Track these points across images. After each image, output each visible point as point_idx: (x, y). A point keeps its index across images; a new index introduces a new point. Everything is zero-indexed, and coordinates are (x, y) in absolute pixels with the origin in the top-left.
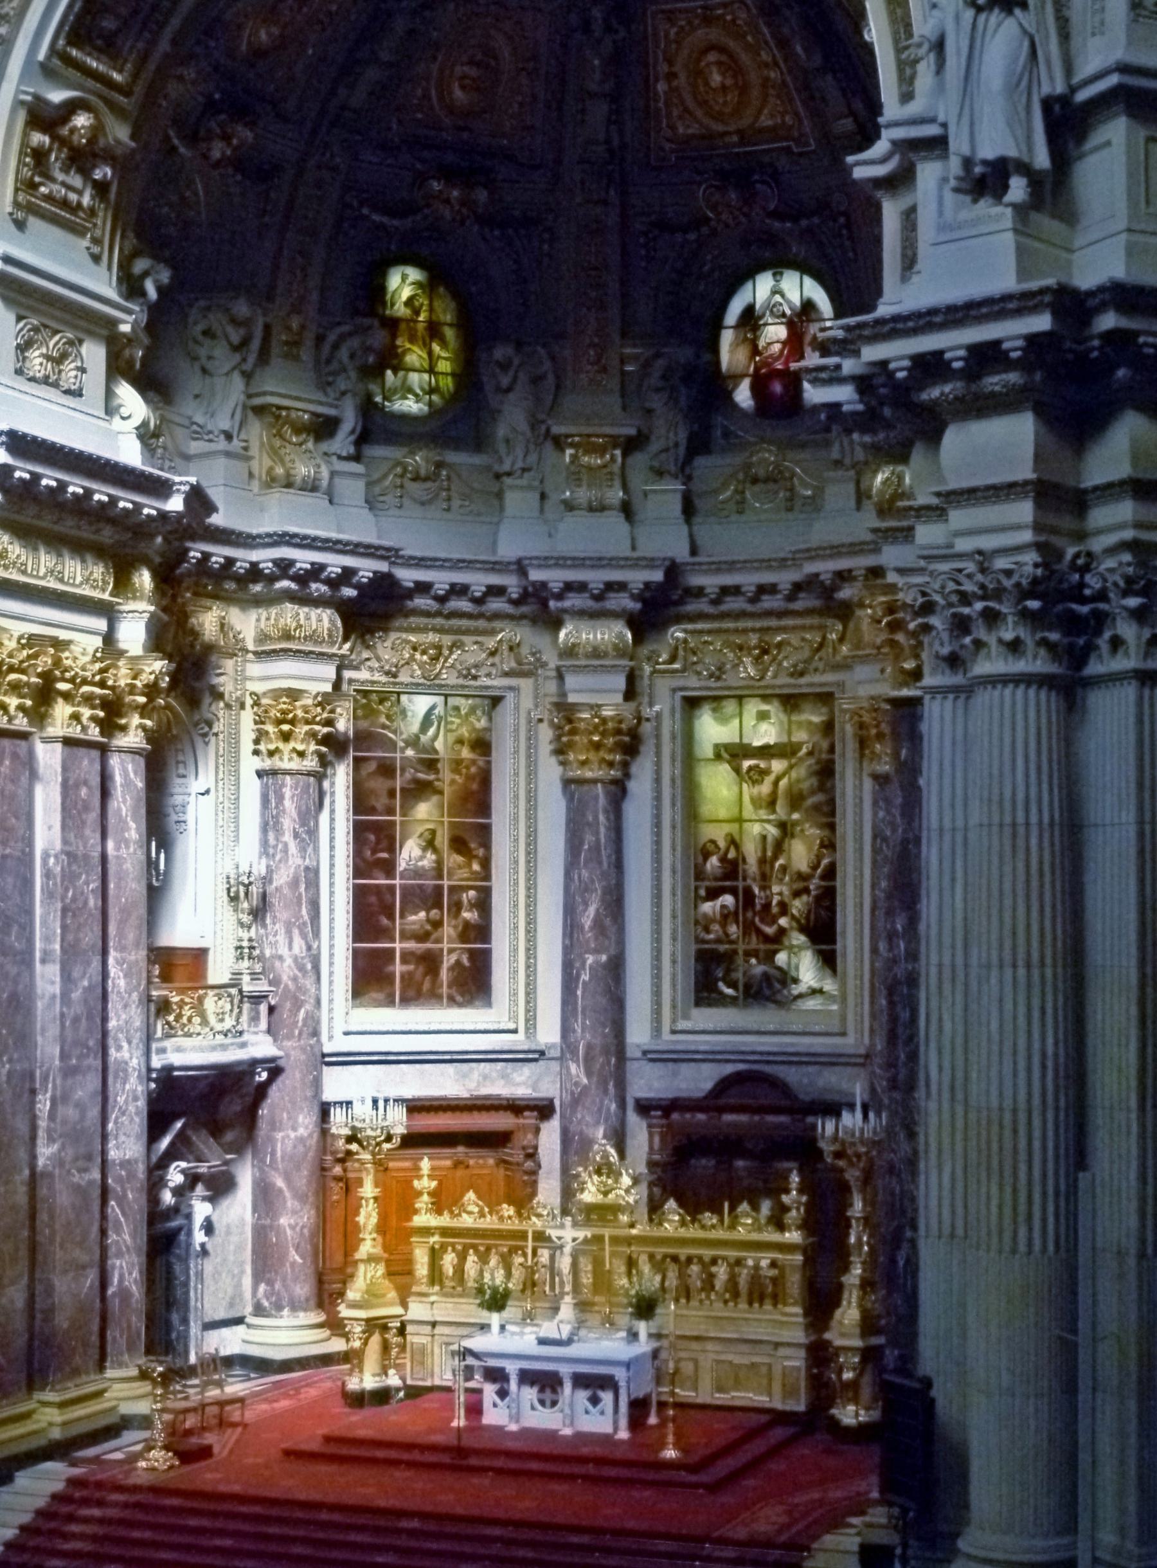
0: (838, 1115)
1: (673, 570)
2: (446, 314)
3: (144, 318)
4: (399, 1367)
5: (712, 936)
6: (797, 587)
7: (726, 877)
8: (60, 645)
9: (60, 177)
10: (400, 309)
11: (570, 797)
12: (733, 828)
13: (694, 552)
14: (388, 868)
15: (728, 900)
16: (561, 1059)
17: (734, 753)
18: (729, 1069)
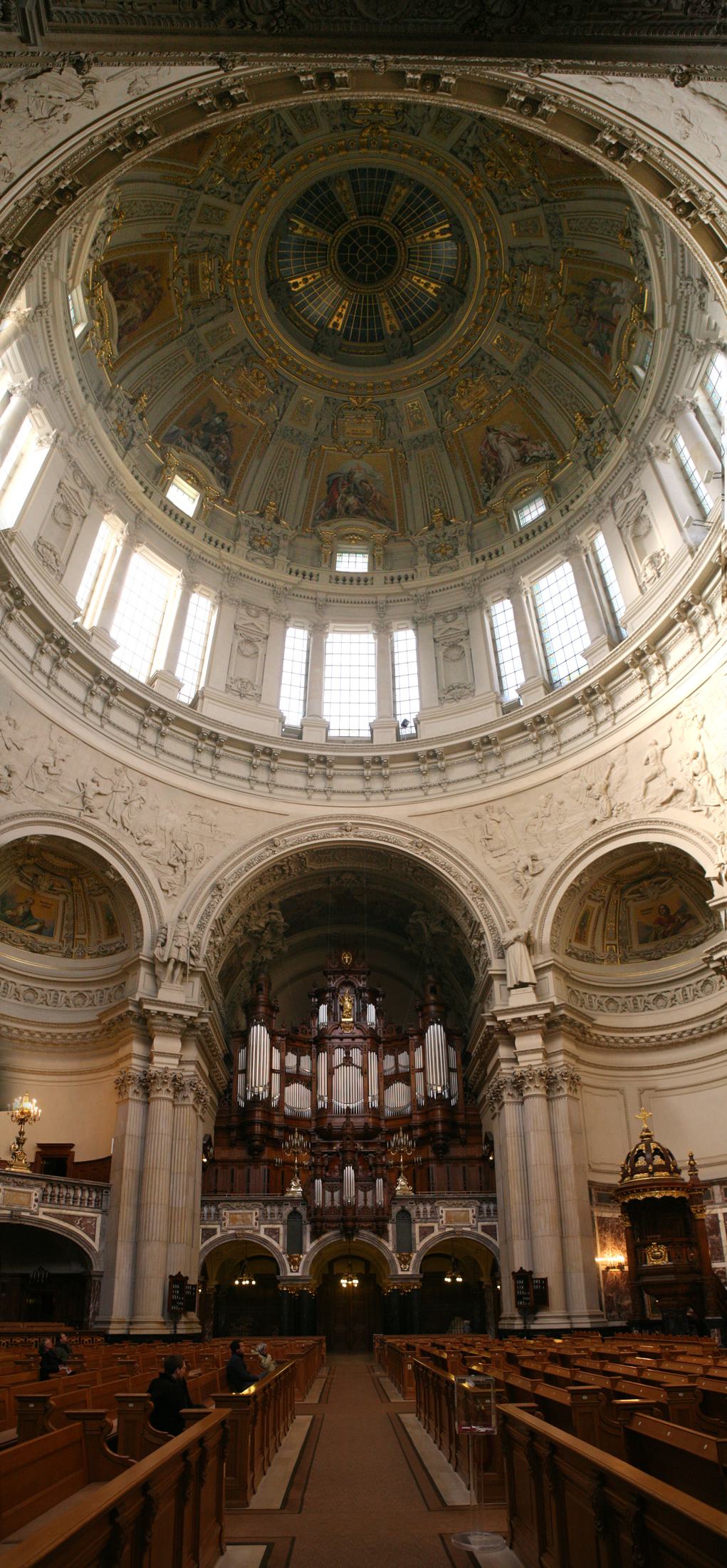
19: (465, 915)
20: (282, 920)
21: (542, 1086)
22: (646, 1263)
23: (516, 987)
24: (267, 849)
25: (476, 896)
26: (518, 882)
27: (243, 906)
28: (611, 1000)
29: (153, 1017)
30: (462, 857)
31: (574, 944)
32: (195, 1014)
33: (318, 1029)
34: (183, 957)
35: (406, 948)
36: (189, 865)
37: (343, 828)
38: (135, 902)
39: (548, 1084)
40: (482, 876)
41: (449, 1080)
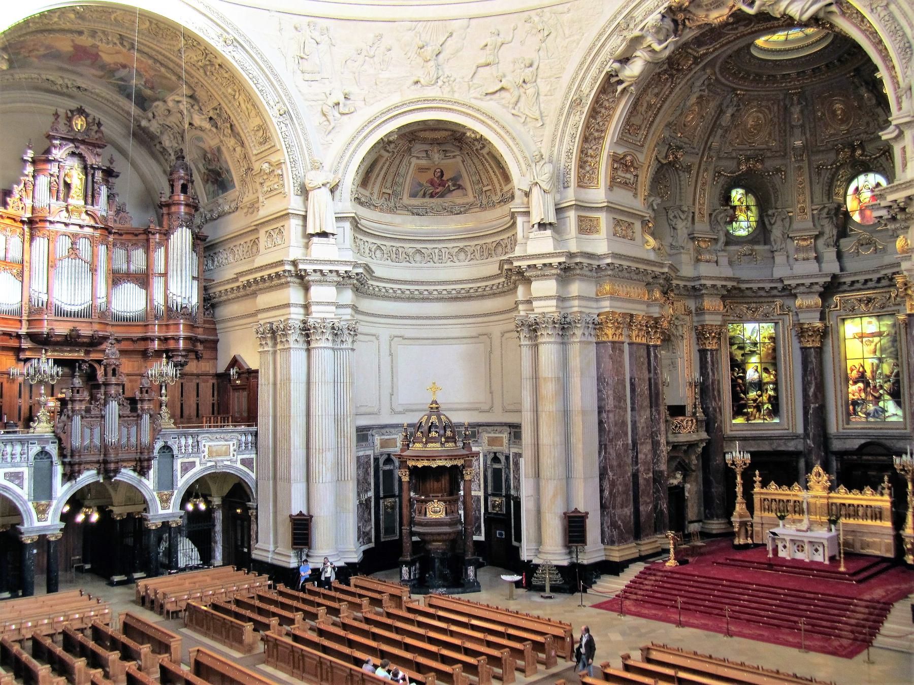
0: (901, 456)
1: (834, 277)
2: (751, 201)
3: (653, 215)
4: (752, 538)
5: (855, 397)
6: (879, 280)
7: (860, 377)
8: (632, 316)
9: (623, 175)
10: (736, 203)
11: (803, 353)
12: (861, 361)
13: (842, 269)
14: (743, 378)
15: (861, 385)
16: (804, 439)
17: (861, 337)
18: (863, 441)
21: (330, 338)
22: (425, 514)
25: (281, 119)
28: (379, 247)
31: (361, 190)
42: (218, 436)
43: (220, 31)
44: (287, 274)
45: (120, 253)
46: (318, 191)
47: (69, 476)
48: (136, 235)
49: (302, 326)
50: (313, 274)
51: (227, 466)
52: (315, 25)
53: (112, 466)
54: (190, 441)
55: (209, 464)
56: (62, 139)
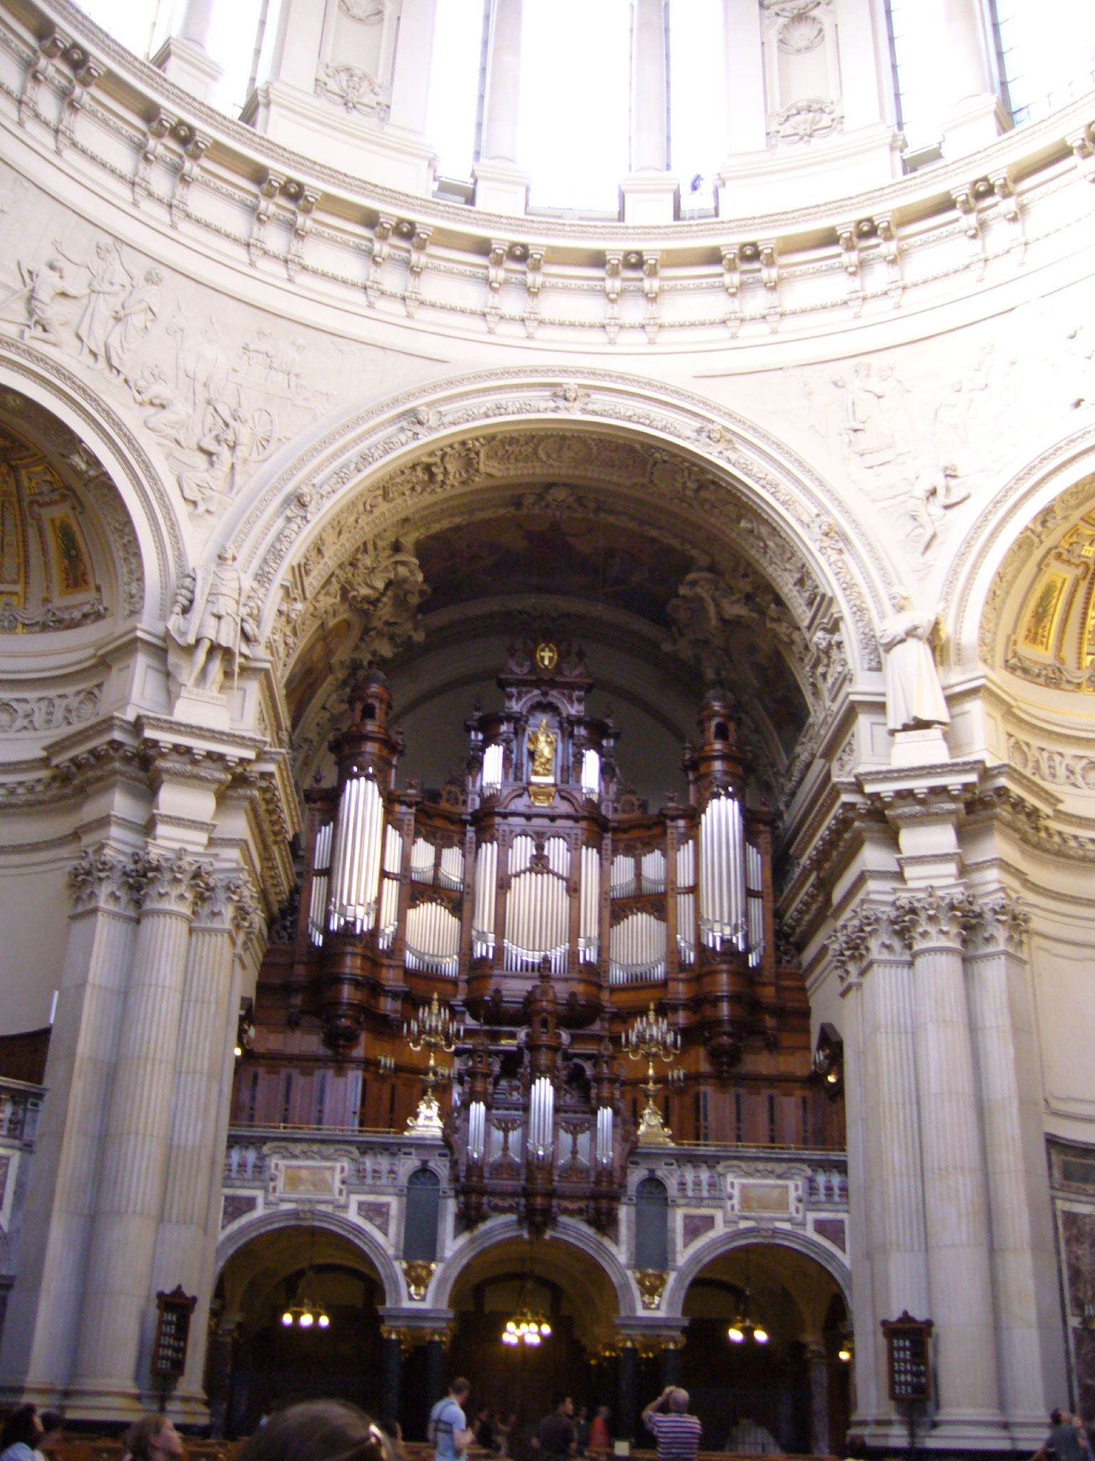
19: (800, 582)
20: (420, 577)
21: (954, 930)
23: (906, 728)
24: (402, 430)
25: (827, 542)
26: (914, 518)
27: (347, 543)
29: (163, 755)
30: (800, 464)
32: (251, 755)
33: (481, 795)
34: (228, 637)
35: (667, 647)
36: (242, 451)
37: (560, 394)
38: (129, 522)
39: (965, 927)
40: (840, 504)
41: (746, 914)
42: (761, 1166)
43: (697, 424)
44: (851, 814)
45: (623, 868)
46: (899, 647)
47: (467, 1220)
48: (649, 828)
49: (893, 914)
50: (901, 802)
51: (786, 1234)
52: (868, 367)
53: (539, 1201)
54: (705, 1175)
55: (744, 1225)
56: (519, 683)
